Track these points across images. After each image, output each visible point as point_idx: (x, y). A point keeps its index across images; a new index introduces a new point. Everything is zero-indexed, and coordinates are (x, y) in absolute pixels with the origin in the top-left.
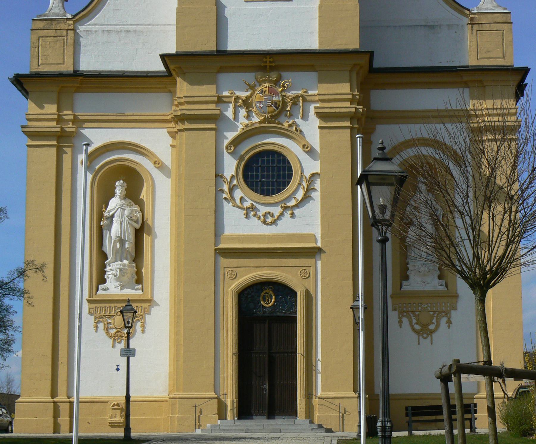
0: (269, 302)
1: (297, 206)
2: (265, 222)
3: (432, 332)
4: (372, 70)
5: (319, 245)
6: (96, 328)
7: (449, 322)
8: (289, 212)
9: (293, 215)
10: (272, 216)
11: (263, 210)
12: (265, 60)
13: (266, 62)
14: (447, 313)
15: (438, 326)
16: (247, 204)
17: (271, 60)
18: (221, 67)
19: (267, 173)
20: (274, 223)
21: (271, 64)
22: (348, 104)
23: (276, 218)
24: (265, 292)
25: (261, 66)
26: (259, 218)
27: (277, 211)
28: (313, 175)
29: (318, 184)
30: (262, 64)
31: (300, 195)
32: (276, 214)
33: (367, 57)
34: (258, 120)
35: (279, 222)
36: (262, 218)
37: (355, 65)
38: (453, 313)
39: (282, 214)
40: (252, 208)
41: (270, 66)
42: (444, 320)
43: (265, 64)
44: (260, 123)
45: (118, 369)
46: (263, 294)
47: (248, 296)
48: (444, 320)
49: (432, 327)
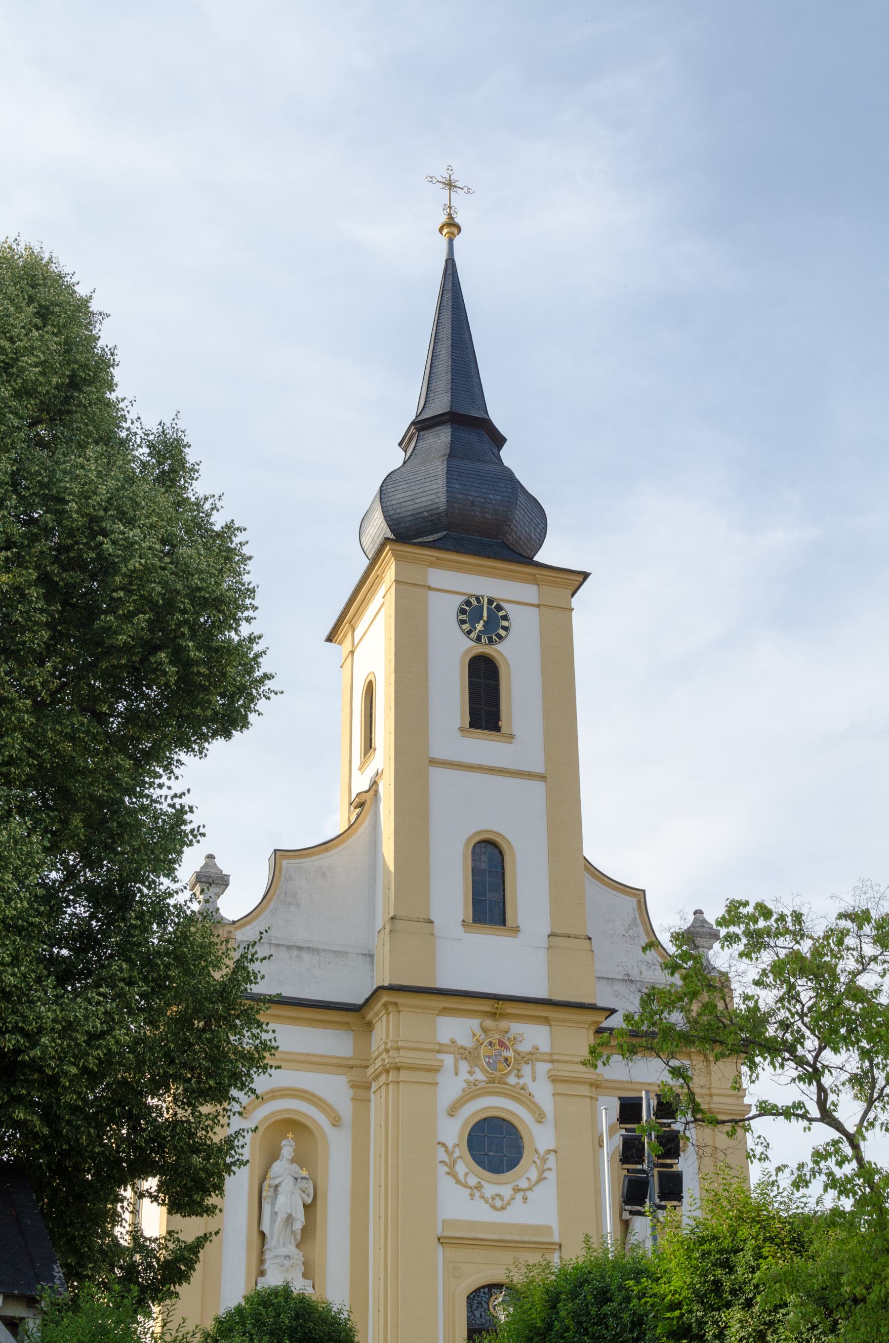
1: (530, 1189)
2: (494, 1207)
5: (556, 1239)
8: (521, 1193)
9: (525, 1199)
10: (502, 1200)
11: (490, 1190)
12: (496, 1005)
16: (472, 1181)
18: (444, 1008)
19: (495, 1146)
20: (503, 1208)
23: (505, 1201)
26: (487, 1202)
27: (506, 1191)
28: (549, 1152)
29: (551, 1162)
30: (493, 1011)
31: (533, 1174)
32: (507, 1197)
34: (484, 1078)
36: (490, 1201)
40: (479, 1187)
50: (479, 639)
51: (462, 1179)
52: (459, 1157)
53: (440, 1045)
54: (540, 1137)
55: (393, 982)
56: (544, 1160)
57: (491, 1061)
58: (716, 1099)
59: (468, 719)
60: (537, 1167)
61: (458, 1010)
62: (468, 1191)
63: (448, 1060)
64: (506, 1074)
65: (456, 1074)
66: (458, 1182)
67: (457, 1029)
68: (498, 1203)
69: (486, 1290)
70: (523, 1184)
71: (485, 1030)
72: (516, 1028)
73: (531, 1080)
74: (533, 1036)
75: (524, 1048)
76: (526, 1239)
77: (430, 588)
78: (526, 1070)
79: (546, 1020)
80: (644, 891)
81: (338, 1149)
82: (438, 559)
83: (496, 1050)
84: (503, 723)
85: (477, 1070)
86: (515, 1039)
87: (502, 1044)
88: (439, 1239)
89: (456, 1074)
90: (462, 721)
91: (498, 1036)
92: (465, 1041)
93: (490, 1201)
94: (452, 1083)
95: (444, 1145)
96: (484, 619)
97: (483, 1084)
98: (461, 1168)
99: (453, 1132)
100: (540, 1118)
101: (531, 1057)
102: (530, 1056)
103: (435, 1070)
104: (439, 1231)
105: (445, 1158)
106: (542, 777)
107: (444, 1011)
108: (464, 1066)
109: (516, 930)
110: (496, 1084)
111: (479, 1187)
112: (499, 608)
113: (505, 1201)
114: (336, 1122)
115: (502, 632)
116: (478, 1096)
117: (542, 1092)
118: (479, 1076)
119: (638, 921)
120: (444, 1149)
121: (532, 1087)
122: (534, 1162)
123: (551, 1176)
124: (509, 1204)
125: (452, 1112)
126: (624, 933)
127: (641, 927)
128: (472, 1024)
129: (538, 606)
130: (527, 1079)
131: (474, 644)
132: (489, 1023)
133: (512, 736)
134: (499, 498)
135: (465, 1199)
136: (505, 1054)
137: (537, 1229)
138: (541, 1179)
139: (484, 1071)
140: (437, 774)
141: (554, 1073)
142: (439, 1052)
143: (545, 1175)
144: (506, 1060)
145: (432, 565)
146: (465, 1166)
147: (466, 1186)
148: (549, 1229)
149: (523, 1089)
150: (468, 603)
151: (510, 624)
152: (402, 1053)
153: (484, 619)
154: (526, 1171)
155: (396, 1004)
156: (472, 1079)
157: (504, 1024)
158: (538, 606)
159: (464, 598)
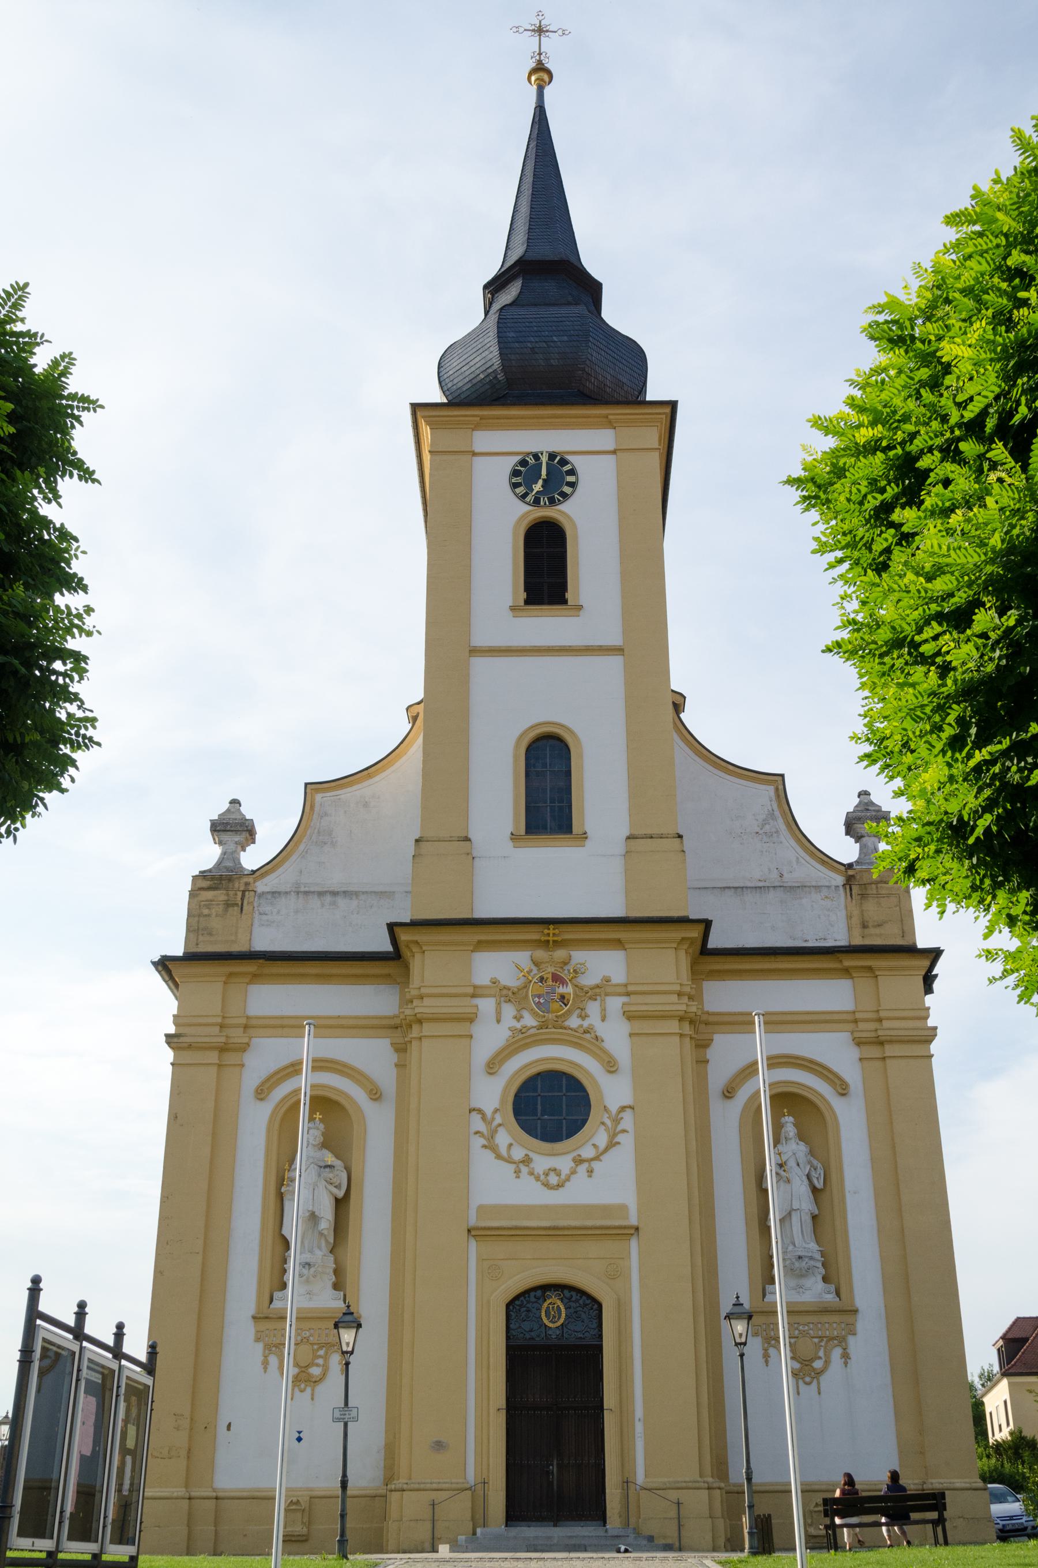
0: (553, 1316)
1: (597, 1158)
2: (547, 1185)
3: (819, 1373)
4: (705, 951)
5: (633, 1221)
6: (265, 1364)
7: (846, 1356)
8: (585, 1165)
9: (590, 1172)
10: (559, 1175)
11: (541, 1163)
12: (546, 931)
13: (548, 935)
14: (842, 1341)
15: (827, 1363)
16: (518, 1153)
17: (557, 931)
18: (480, 942)
20: (559, 1186)
21: (555, 939)
22: (674, 998)
23: (563, 1177)
24: (548, 1301)
25: (540, 941)
26: (538, 1179)
27: (564, 1164)
28: (623, 1109)
29: (628, 1121)
30: (543, 938)
31: (601, 1139)
33: (702, 927)
34: (534, 1023)
35: (567, 1184)
36: (542, 1177)
37: (683, 939)
38: (851, 1339)
39: (573, 1172)
40: (527, 1161)
41: (554, 941)
42: (837, 1353)
43: (546, 938)
44: (540, 1028)
45: (299, 1439)
46: (546, 1305)
47: (521, 1306)
48: (837, 1353)
49: (818, 1364)
50: (536, 502)
51: (504, 1151)
52: (500, 1125)
53: (475, 987)
54: (612, 1092)
55: (414, 918)
56: (617, 1121)
57: (542, 1001)
58: (886, 1024)
59: (523, 595)
60: (607, 1129)
61: (500, 942)
62: (513, 1166)
63: (486, 1005)
64: (563, 1015)
65: (498, 1021)
66: (499, 1156)
67: (500, 966)
68: (553, 1179)
69: (539, 1293)
70: (588, 1152)
71: (536, 964)
72: (579, 956)
73: (599, 1019)
74: (601, 965)
75: (588, 980)
76: (589, 1223)
77: (474, 454)
78: (593, 1008)
79: (618, 944)
80: (782, 776)
81: (377, 1130)
82: (482, 418)
83: (548, 986)
84: (569, 595)
85: (526, 1014)
86: (575, 971)
87: (557, 978)
88: (469, 1231)
89: (498, 1021)
90: (515, 599)
91: (551, 969)
92: (510, 979)
93: (542, 1177)
94: (491, 1033)
95: (480, 1111)
96: (545, 479)
97: (533, 1031)
98: (503, 1139)
99: (492, 1094)
100: (611, 1066)
101: (601, 990)
102: (598, 990)
103: (471, 1019)
104: (473, 1221)
105: (482, 1127)
106: (618, 650)
107: (481, 946)
108: (509, 1011)
109: (584, 836)
110: (552, 1028)
111: (527, 1161)
112: (564, 462)
113: (563, 1177)
114: (376, 1095)
115: (567, 490)
116: (527, 1046)
117: (615, 1035)
118: (529, 1020)
119: (777, 813)
120: (480, 1116)
121: (602, 1029)
122: (603, 1123)
123: (627, 1141)
124: (568, 1179)
125: (492, 1067)
126: (757, 829)
127: (780, 821)
128: (523, 957)
129: (614, 452)
130: (594, 1019)
131: (531, 508)
132: (540, 954)
133: (580, 607)
134: (566, 338)
135: (509, 1177)
136: (561, 990)
137: (606, 1210)
138: (612, 1144)
139: (534, 1014)
140: (480, 665)
142: (474, 996)
143: (616, 1140)
144: (562, 997)
145: (477, 427)
146: (509, 1136)
147: (509, 1160)
148: (623, 1208)
150: (523, 463)
151: (577, 479)
152: (427, 1001)
153: (545, 479)
154: (594, 1135)
155: (417, 942)
156: (518, 1026)
157: (560, 954)
158: (614, 452)
159: (518, 458)
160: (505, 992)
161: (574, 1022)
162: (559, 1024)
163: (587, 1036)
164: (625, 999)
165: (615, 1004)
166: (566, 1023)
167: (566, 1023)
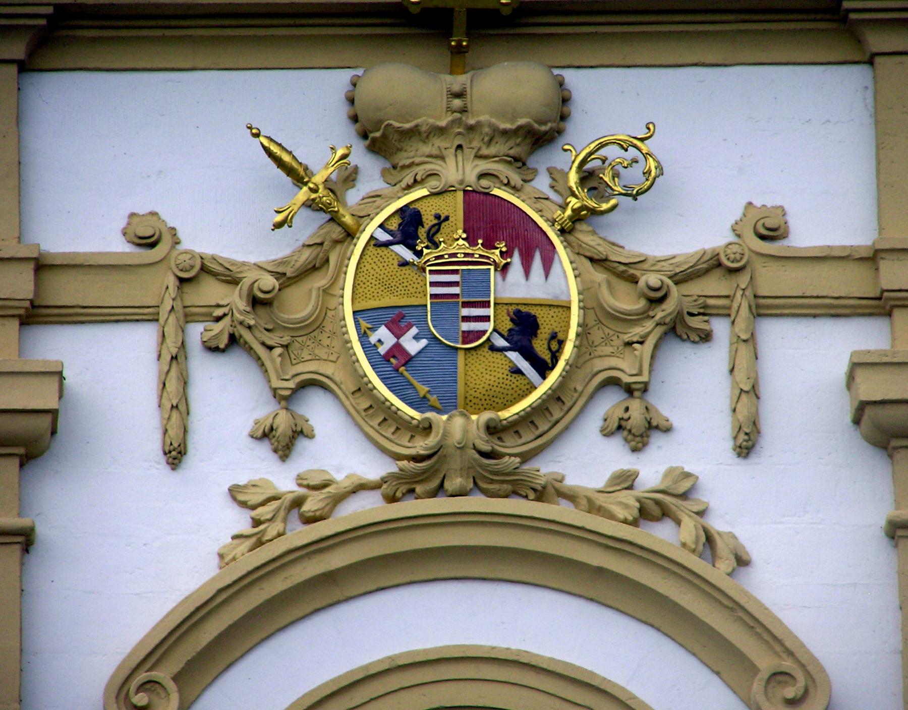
34: (374, 468)
44: (397, 488)
53: (42, 266)
57: (412, 345)
64: (528, 419)
65: (175, 455)
71: (382, 137)
72: (617, 100)
73: (724, 445)
75: (673, 233)
78: (694, 387)
85: (322, 414)
86: (588, 177)
87: (495, 224)
89: (175, 455)
91: (459, 170)
92: (234, 222)
102: (713, 286)
108: (229, 398)
116: (330, 589)
118: (341, 451)
121: (736, 500)
132: (405, 82)
136: (518, 285)
139: (374, 417)
141: (874, 387)
142: (34, 315)
144: (524, 326)
149: (652, 511)
156: (283, 479)
157: (508, 84)
160: (211, 293)
161: (586, 460)
162: (501, 463)
163: (662, 536)
164: (865, 336)
165: (811, 362)
166: (546, 467)
167: (546, 467)
